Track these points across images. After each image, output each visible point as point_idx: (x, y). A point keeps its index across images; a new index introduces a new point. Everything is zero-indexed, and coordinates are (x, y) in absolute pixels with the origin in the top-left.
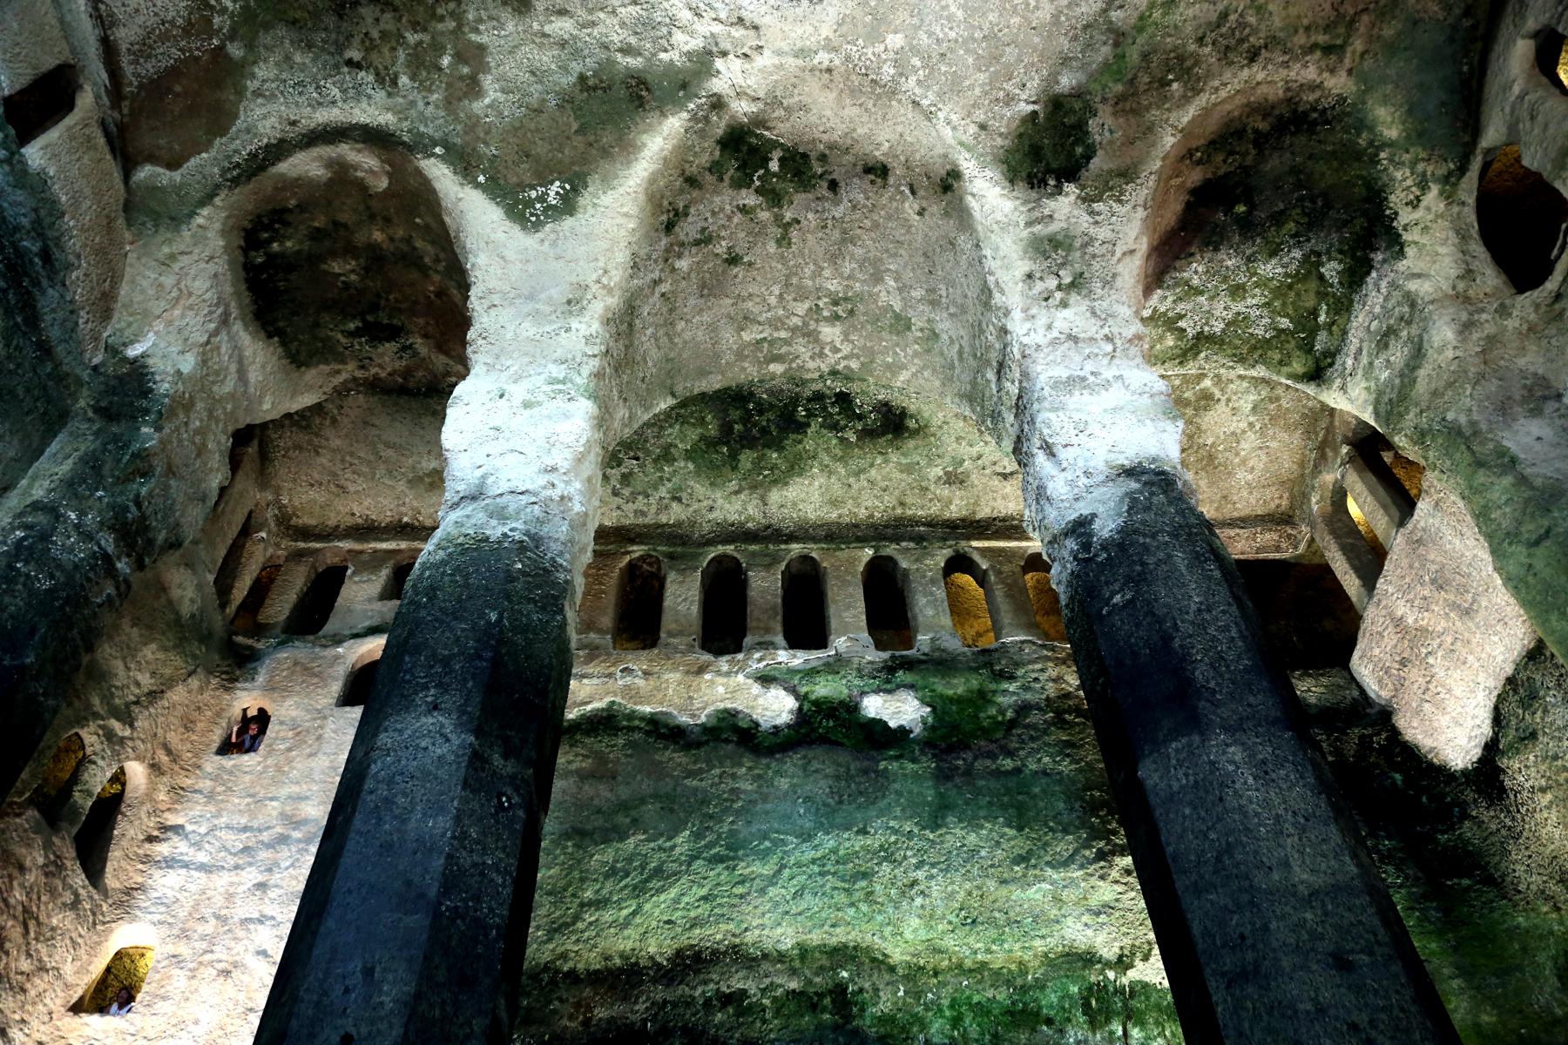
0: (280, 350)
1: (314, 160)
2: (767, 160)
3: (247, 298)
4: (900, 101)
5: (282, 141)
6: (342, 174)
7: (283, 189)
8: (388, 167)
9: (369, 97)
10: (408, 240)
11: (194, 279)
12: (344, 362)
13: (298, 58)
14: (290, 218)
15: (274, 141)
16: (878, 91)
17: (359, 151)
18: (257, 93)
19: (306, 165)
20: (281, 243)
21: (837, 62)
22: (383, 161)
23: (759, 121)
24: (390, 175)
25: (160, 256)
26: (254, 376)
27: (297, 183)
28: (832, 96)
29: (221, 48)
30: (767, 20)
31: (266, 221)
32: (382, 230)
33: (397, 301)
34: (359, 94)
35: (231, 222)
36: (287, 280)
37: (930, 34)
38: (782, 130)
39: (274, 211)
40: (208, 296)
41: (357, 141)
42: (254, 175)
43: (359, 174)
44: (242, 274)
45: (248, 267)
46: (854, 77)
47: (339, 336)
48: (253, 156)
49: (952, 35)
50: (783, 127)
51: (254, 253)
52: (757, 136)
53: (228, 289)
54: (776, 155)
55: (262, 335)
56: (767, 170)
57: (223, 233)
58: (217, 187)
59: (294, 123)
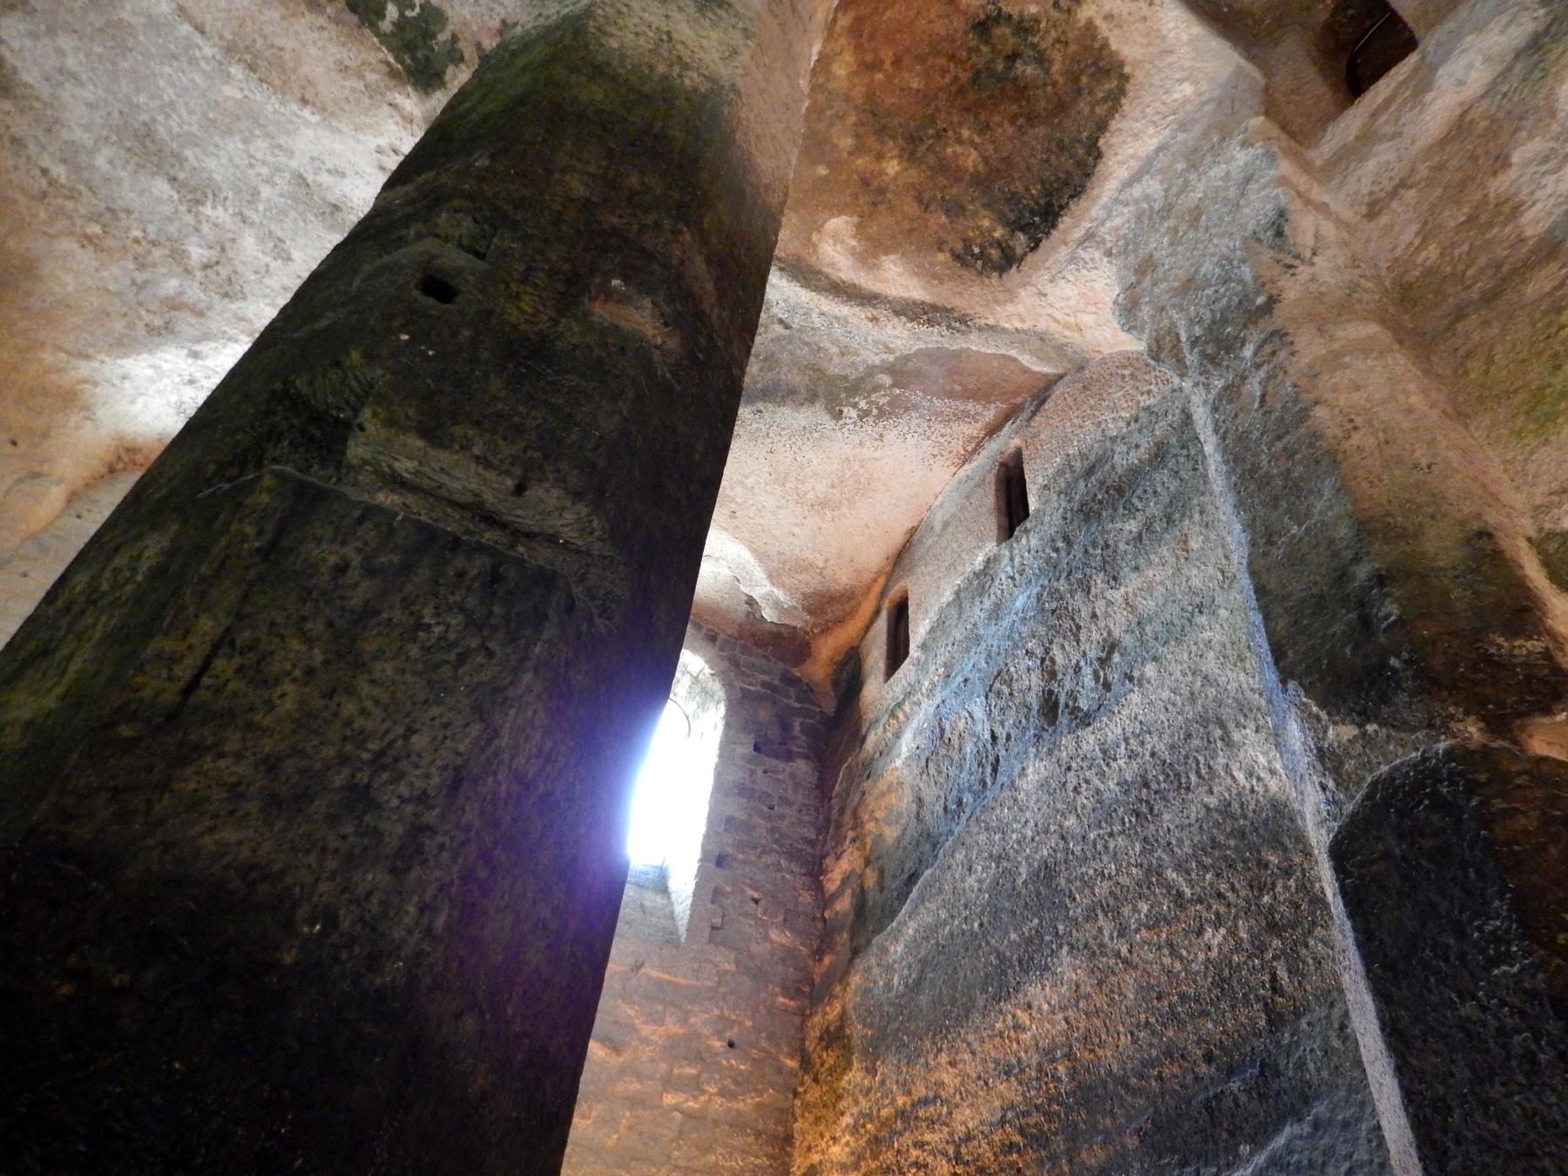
0: (1113, 125)
1: (886, 281)
2: (401, 25)
3: (1065, 222)
4: (221, 37)
5: (897, 313)
6: (872, 249)
7: (936, 277)
8: (815, 237)
9: (785, 301)
10: (857, 150)
11: (1068, 299)
12: (1090, 26)
13: (834, 350)
14: (959, 247)
15: (904, 319)
16: (248, 57)
17: (832, 265)
18: (889, 350)
19: (897, 278)
20: (991, 230)
21: (295, 107)
22: (815, 246)
23: (393, 74)
24: (819, 228)
25: (1076, 335)
26: (1150, 141)
27: (921, 272)
28: (305, 69)
29: (894, 385)
30: (369, 170)
31: (980, 263)
32: (882, 173)
33: (945, 72)
34: (793, 308)
35: (1001, 296)
36: (1028, 190)
37: (193, 81)
38: (373, 55)
39: (965, 264)
40: (1071, 278)
41: (827, 277)
42: (947, 310)
43: (853, 243)
44: (1044, 244)
45: (1035, 245)
46: (277, 82)
47: (1056, 67)
48: (930, 322)
49: (167, 70)
50: (373, 57)
51: (1019, 251)
52: (402, 63)
53: (1064, 252)
54: (386, 26)
55: (1100, 167)
56: (402, 14)
57: (1012, 296)
58: (980, 329)
59: (874, 319)
